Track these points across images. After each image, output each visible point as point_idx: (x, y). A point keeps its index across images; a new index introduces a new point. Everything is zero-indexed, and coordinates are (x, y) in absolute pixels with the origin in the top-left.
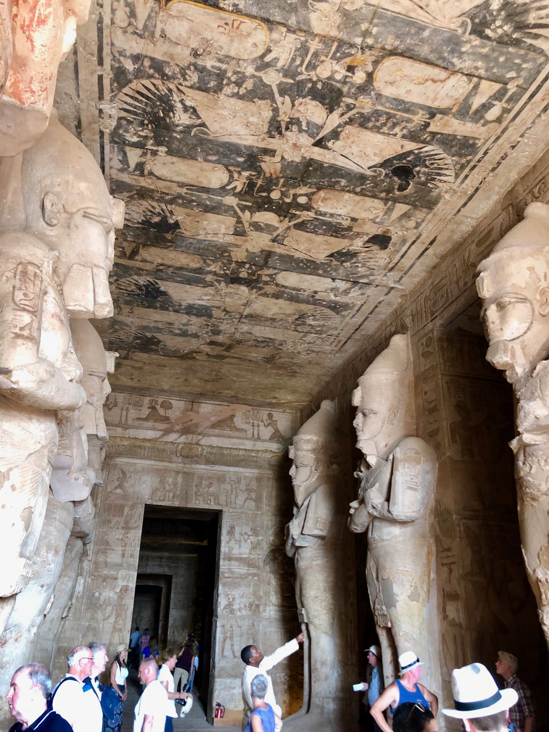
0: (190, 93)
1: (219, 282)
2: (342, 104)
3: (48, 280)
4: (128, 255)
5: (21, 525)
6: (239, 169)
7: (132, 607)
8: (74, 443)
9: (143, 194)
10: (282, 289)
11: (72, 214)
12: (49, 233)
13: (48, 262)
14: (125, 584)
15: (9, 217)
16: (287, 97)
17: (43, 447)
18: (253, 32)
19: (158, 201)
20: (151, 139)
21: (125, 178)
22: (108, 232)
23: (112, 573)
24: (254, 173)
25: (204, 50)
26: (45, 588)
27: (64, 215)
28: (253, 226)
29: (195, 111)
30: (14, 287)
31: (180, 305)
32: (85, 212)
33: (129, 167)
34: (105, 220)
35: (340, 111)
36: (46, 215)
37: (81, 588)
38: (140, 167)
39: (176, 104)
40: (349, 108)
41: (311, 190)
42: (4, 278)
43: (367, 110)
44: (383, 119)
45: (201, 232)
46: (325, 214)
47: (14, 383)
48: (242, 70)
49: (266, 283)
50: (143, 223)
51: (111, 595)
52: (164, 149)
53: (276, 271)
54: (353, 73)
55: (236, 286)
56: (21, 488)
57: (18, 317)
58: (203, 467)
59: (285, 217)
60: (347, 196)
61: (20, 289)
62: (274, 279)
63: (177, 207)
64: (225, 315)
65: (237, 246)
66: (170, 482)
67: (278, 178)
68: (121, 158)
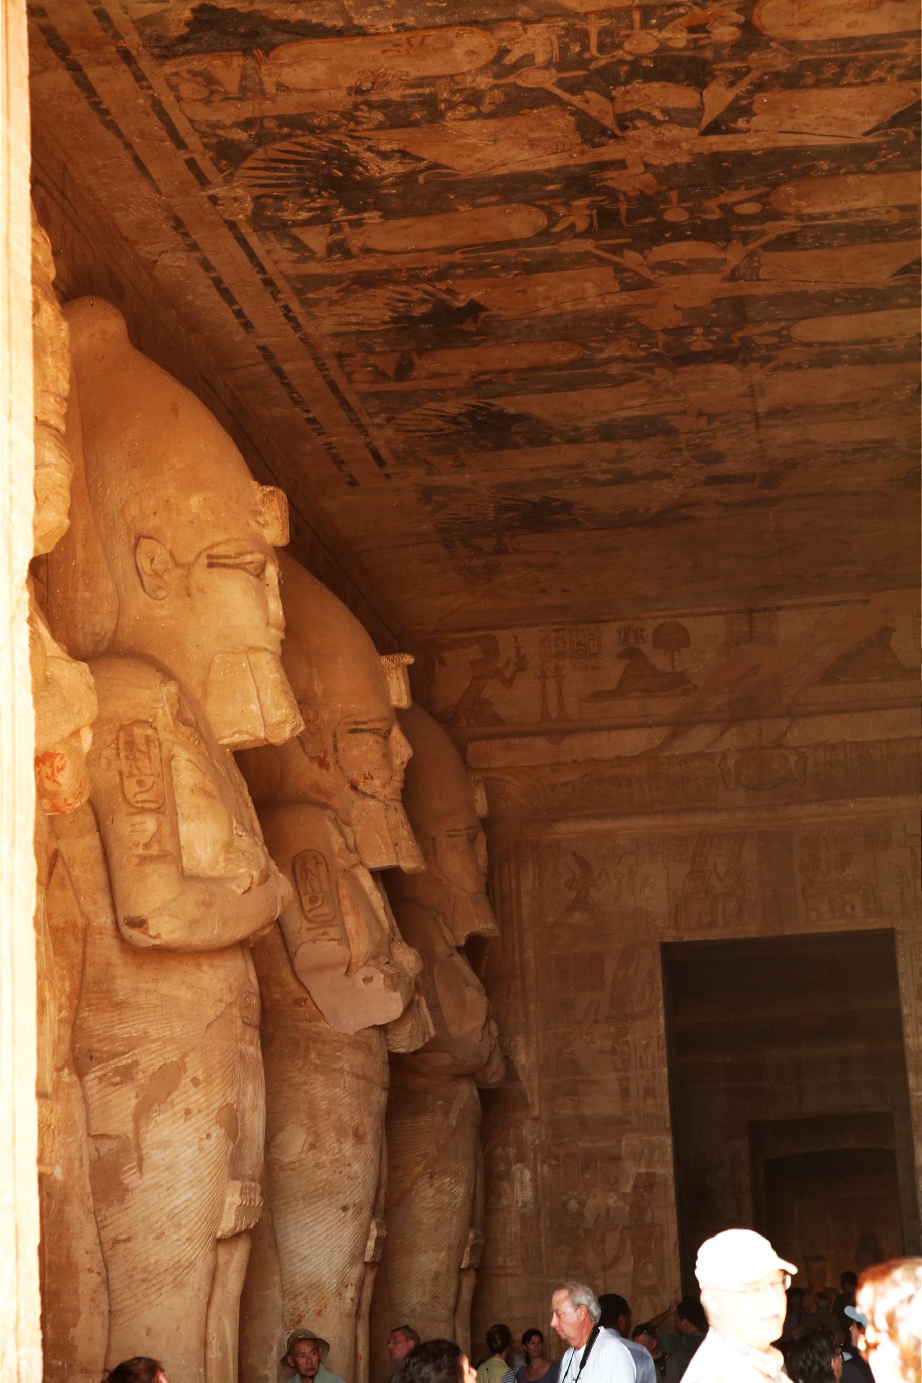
0: (381, 134)
1: (651, 370)
2: (717, 73)
3: (170, 737)
4: (392, 376)
5: (217, 1132)
6: (561, 200)
7: (673, 1229)
8: (346, 904)
9: (368, 281)
10: (827, 348)
11: (188, 567)
12: (159, 613)
13: (163, 708)
14: (642, 1170)
15: (88, 594)
16: (586, 93)
17: (230, 1005)
18: (456, 40)
19: (407, 283)
20: (338, 207)
21: (313, 268)
22: (260, 573)
23: (603, 1144)
24: (600, 198)
25: (374, 84)
26: (351, 1212)
27: (178, 573)
28: (660, 269)
29: (404, 154)
30: (121, 773)
31: (577, 429)
32: (210, 557)
33: (313, 253)
34: (249, 558)
35: (721, 81)
36: (145, 584)
37: (529, 1193)
38: (340, 249)
39: (361, 155)
40: (738, 75)
41: (755, 192)
42: (104, 761)
43: (781, 63)
44: (830, 71)
45: (540, 305)
46: (825, 216)
47: (155, 938)
48: (468, 85)
49: (775, 347)
50: (394, 320)
51: (610, 1202)
52: (376, 213)
53: (783, 324)
54: (709, 32)
55: (700, 368)
56: (206, 1080)
57: (137, 827)
58: (813, 808)
59: (729, 240)
60: (851, 179)
61: (131, 775)
62: (790, 339)
63: (459, 281)
64: (710, 423)
65: (645, 306)
66: (722, 870)
67: (658, 193)
68: (289, 245)
